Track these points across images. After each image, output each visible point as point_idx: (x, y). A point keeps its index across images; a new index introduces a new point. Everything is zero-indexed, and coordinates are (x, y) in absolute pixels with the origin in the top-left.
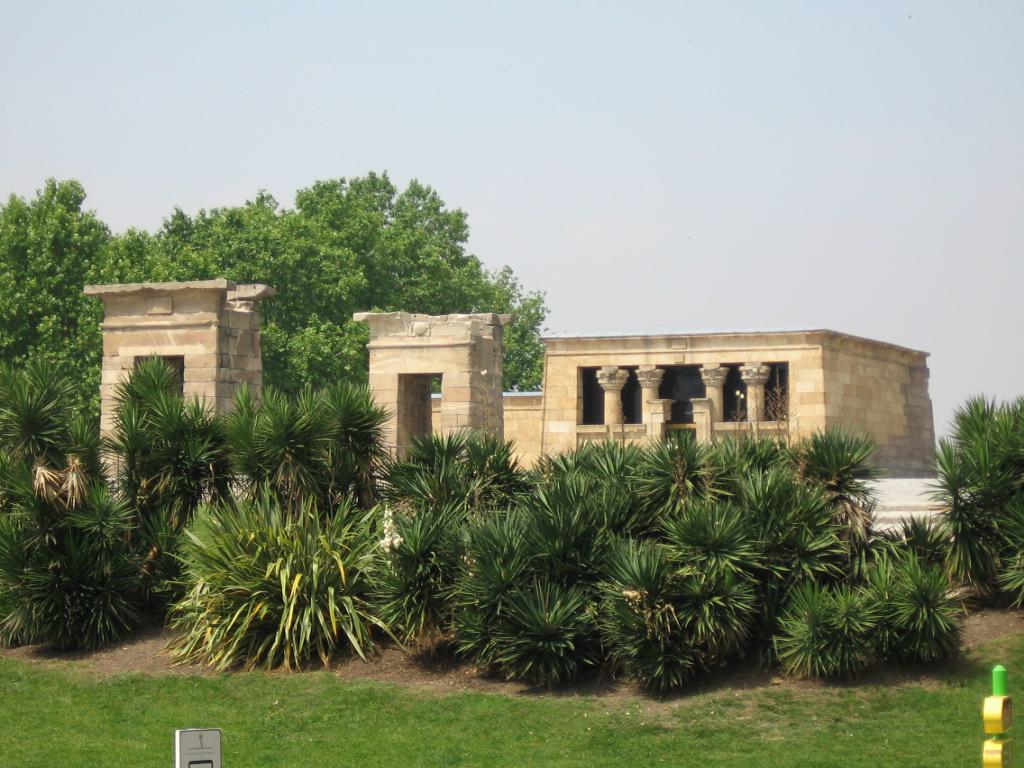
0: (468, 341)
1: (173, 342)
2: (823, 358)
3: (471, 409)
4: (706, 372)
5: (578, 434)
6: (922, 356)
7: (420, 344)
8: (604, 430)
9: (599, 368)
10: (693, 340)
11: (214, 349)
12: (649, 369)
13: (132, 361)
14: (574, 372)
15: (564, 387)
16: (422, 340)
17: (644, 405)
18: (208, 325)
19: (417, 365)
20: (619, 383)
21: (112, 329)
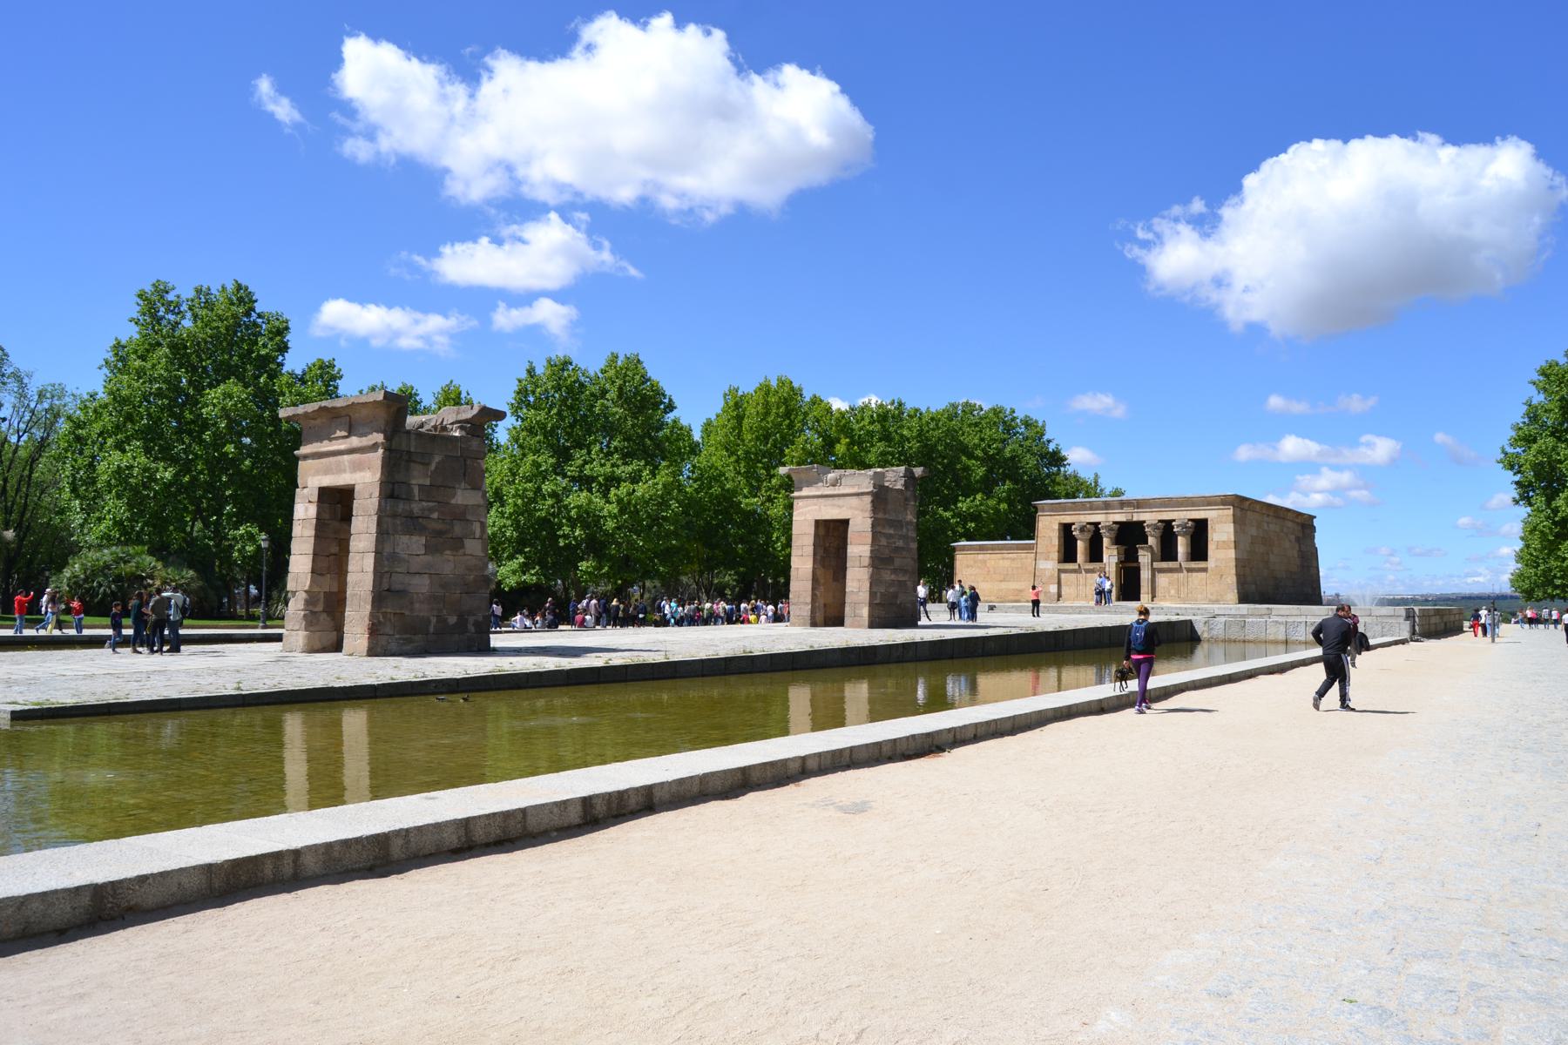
0: (871, 489)
2: (1234, 515)
3: (872, 551)
5: (1059, 570)
6: (1312, 517)
8: (1077, 567)
9: (1074, 524)
10: (1139, 504)
11: (378, 475)
12: (1107, 524)
14: (1056, 527)
15: (1050, 537)
16: (835, 490)
17: (1104, 548)
18: (374, 447)
19: (831, 512)
20: (1088, 536)
21: (306, 457)
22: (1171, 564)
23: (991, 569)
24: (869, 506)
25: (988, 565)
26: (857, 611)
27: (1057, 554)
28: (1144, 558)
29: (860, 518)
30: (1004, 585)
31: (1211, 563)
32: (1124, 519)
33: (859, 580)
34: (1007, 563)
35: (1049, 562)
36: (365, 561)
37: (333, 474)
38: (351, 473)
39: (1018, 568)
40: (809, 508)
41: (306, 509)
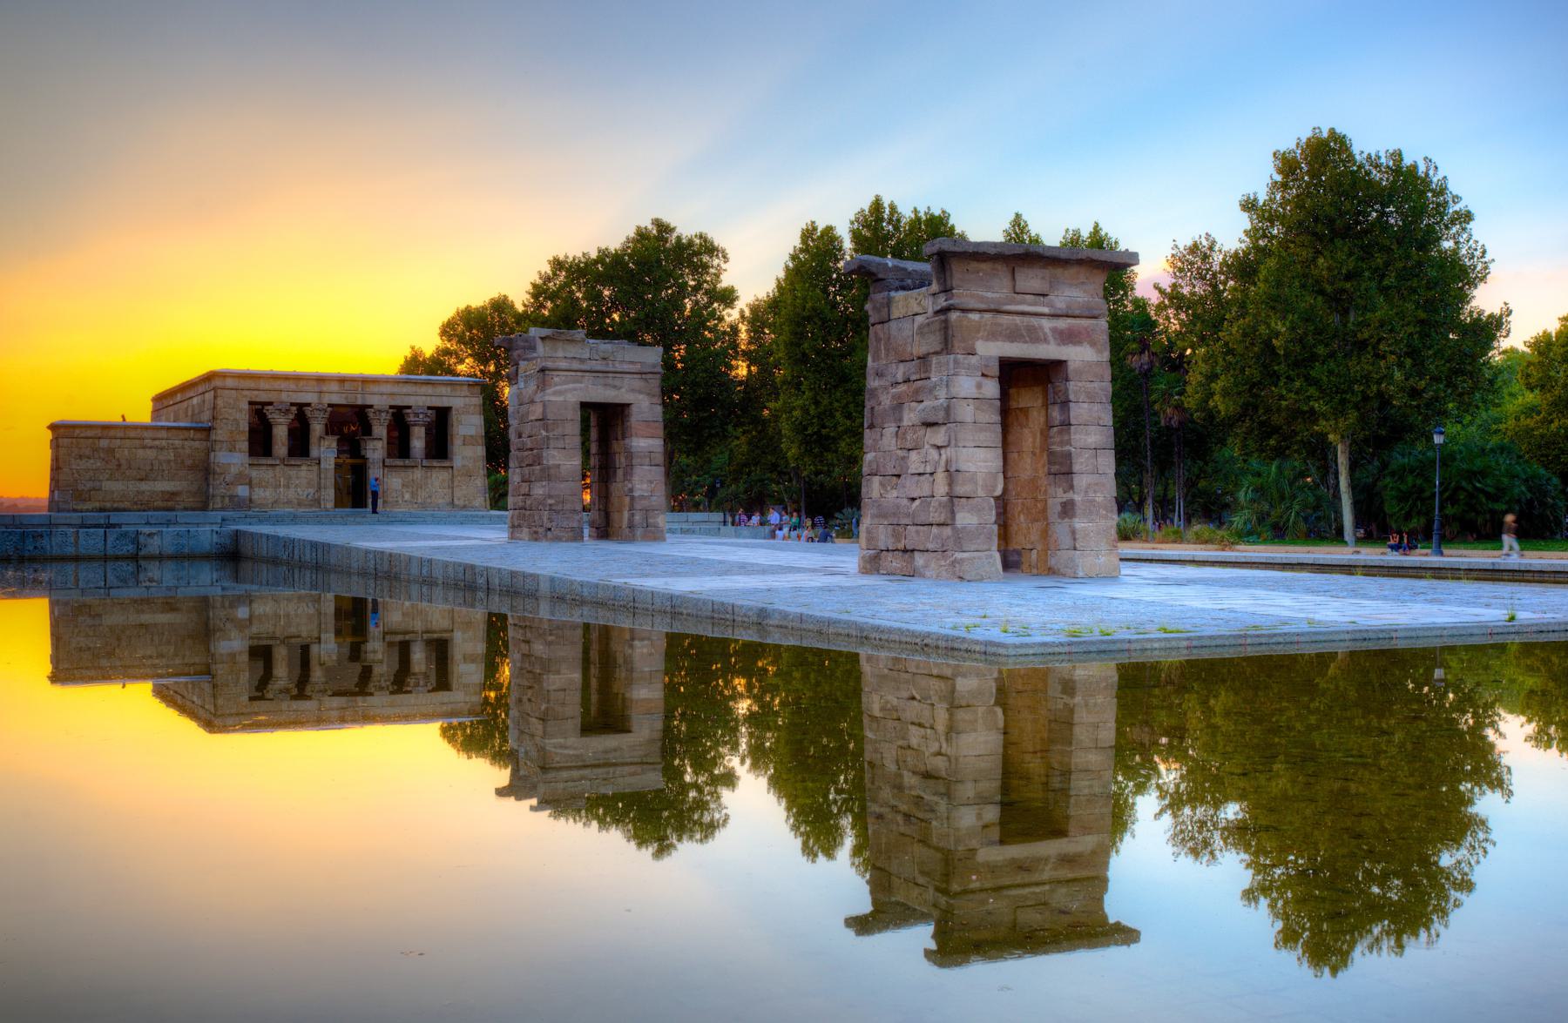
4: (380, 411)
7: (608, 369)
13: (997, 364)
14: (246, 406)
15: (235, 419)
22: (407, 462)
23: (123, 462)
24: (657, 391)
25: (117, 455)
26: (651, 521)
27: (247, 443)
28: (375, 450)
29: (647, 403)
30: (144, 486)
31: (458, 461)
32: (343, 402)
33: (651, 482)
34: (151, 454)
35: (236, 454)
37: (1026, 342)
38: (1059, 345)
39: (169, 461)
40: (571, 386)
41: (979, 386)
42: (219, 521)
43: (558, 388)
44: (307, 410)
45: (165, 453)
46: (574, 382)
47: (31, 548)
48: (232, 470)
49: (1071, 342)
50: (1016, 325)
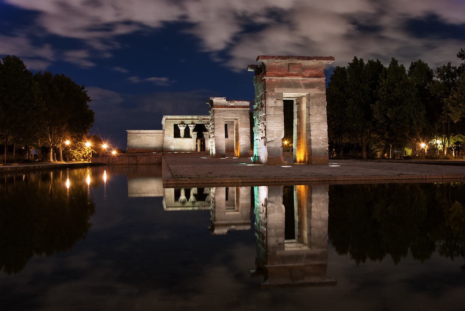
1: (303, 87)
15: (171, 128)
23: (143, 140)
25: (142, 138)
36: (321, 126)
37: (293, 88)
38: (306, 88)
40: (222, 113)
41: (275, 102)
42: (162, 155)
43: (218, 114)
44: (189, 125)
45: (153, 137)
46: (222, 112)
47: (111, 162)
48: (170, 141)
49: (311, 88)
50: (290, 83)
